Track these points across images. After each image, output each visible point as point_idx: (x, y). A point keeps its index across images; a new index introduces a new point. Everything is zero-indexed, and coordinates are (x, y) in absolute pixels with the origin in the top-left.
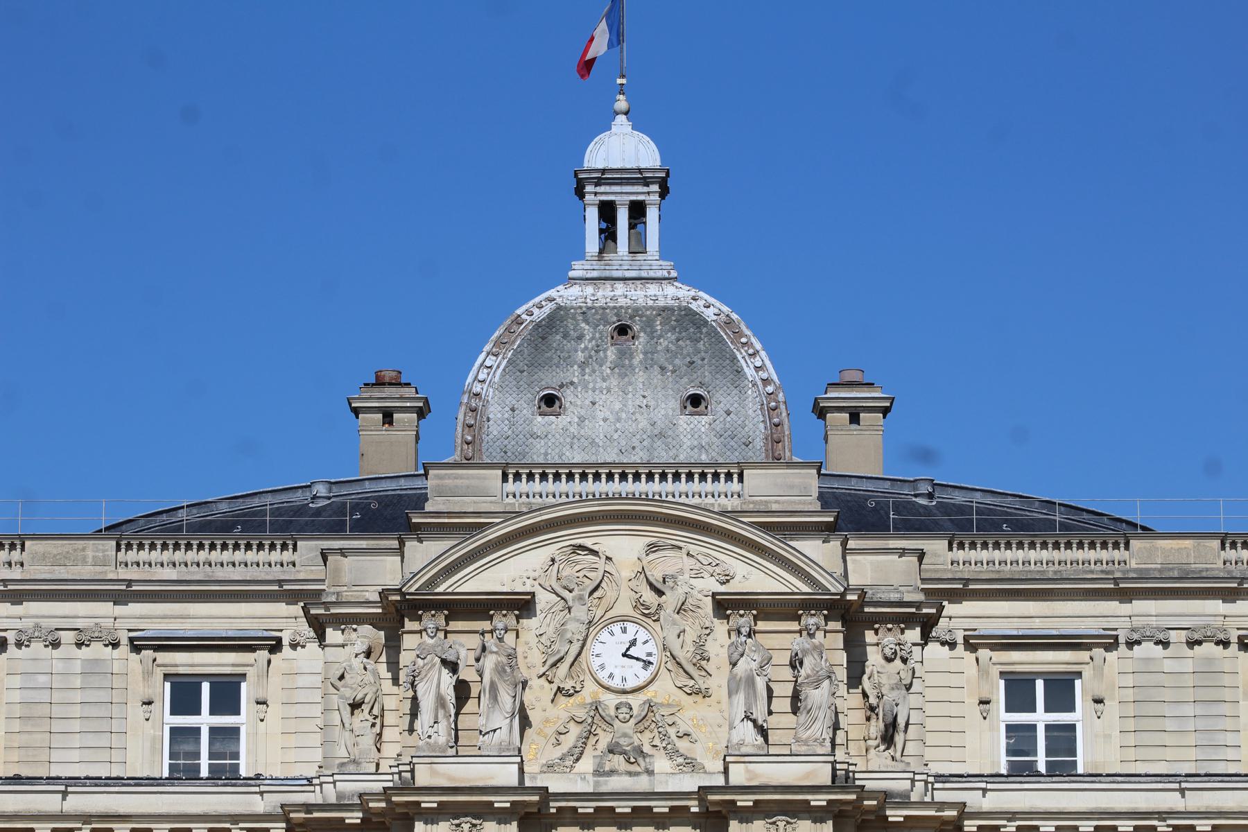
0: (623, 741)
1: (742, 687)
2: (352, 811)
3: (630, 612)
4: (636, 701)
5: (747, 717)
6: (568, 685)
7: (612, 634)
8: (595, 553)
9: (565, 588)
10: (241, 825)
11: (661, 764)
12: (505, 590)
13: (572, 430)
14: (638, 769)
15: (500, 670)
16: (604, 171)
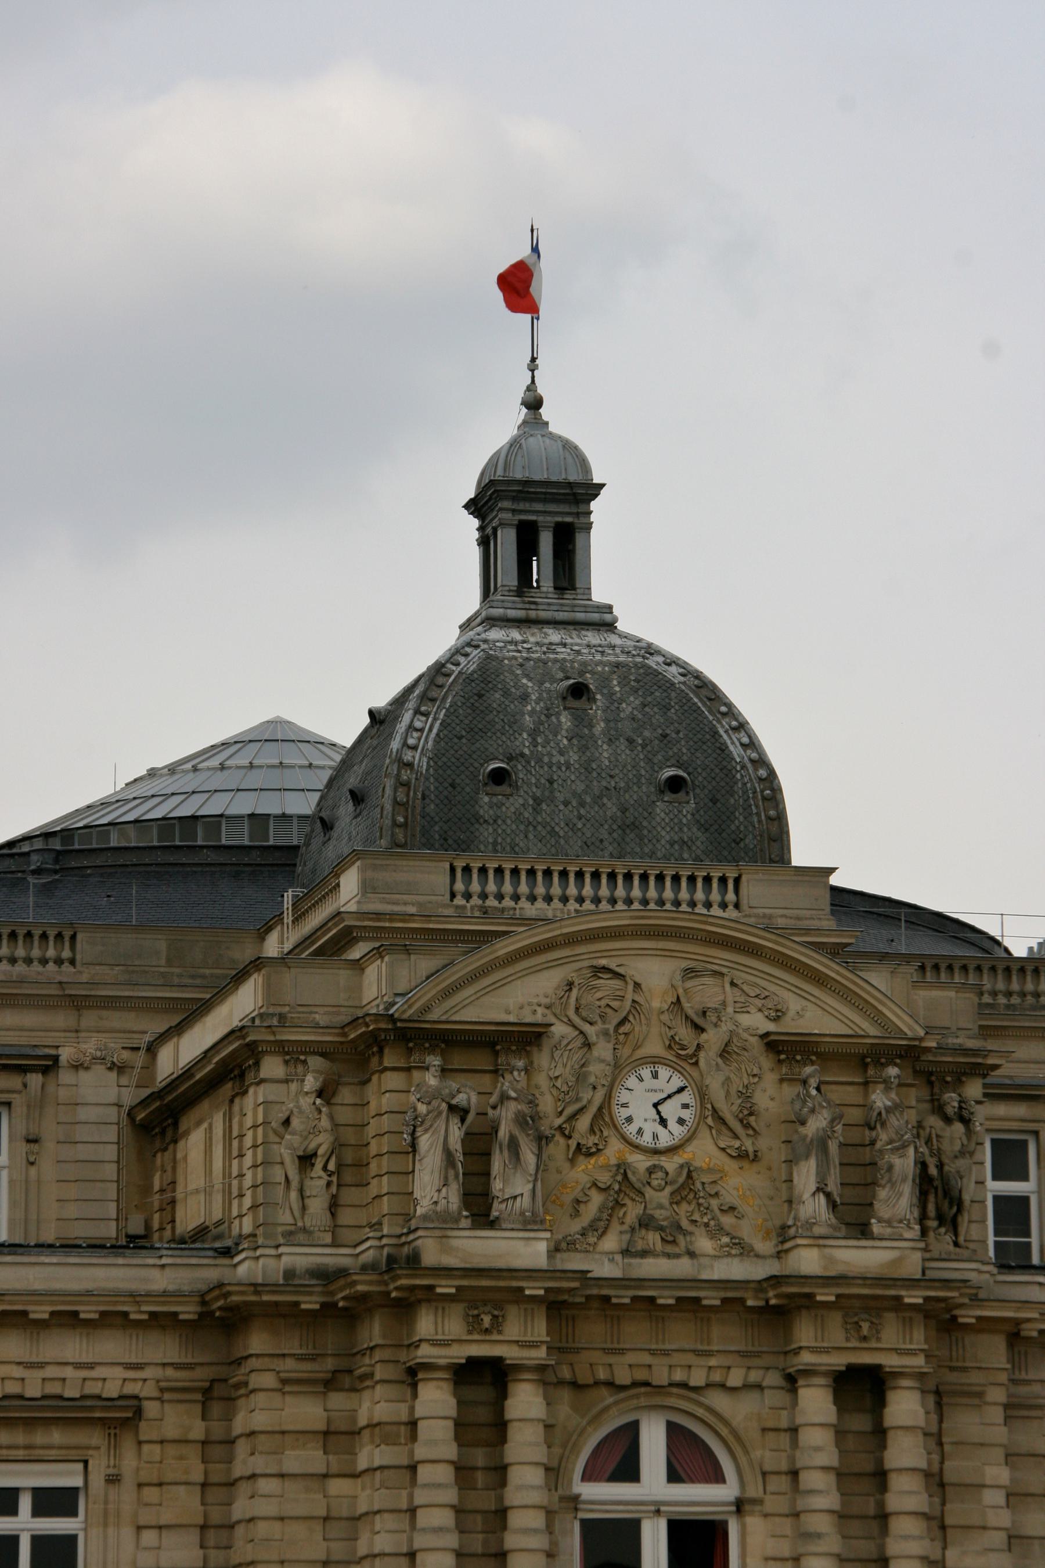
0: (658, 1214)
1: (814, 1152)
2: (310, 1294)
4: (671, 1164)
7: (641, 1080)
9: (584, 1020)
10: (144, 1308)
11: (704, 1244)
12: (512, 1019)
13: (526, 815)
14: (677, 1250)
15: (521, 1121)
16: (527, 483)
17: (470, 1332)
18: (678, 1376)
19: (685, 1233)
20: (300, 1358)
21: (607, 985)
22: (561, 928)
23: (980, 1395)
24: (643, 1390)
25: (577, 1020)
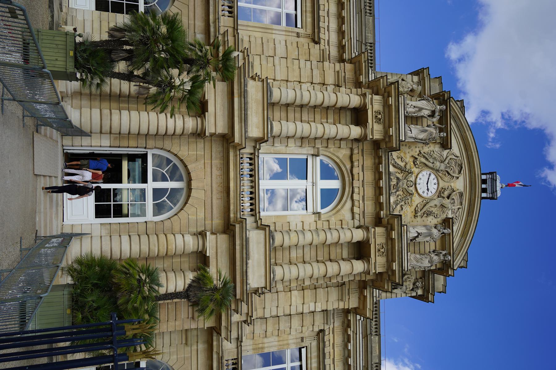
0: (401, 183)
2: (365, 78)
4: (412, 189)
6: (418, 162)
7: (434, 179)
8: (460, 172)
15: (431, 134)
17: (375, 112)
18: (356, 190)
19: (396, 192)
20: (345, 77)
21: (457, 169)
22: (475, 152)
23: (342, 300)
24: (351, 178)
25: (449, 158)
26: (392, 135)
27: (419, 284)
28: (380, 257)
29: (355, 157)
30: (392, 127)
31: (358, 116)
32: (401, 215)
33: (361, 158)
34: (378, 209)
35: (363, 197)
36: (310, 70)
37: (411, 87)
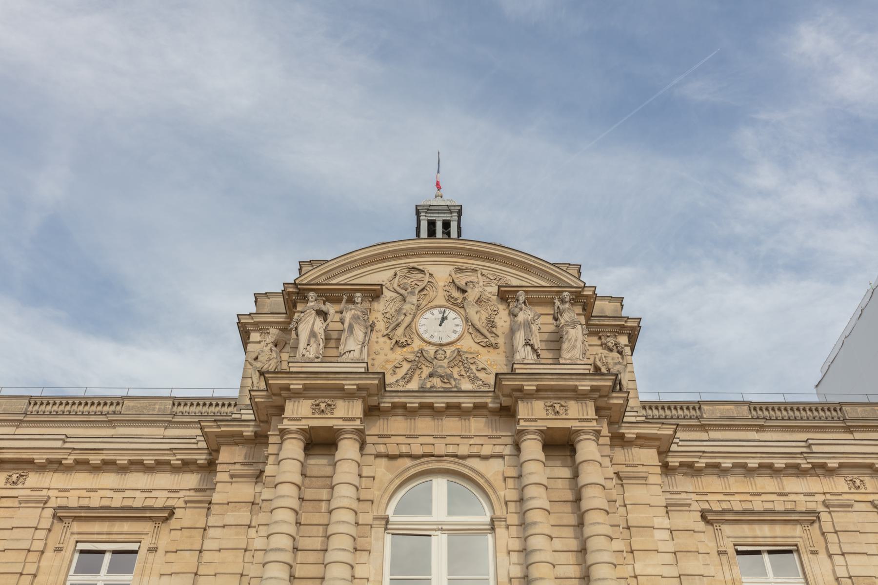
2: (248, 426)
3: (445, 303)
4: (449, 350)
5: (527, 344)
6: (403, 340)
7: (433, 314)
15: (355, 318)
17: (314, 413)
19: (455, 379)
20: (243, 464)
21: (418, 276)
23: (646, 478)
24: (430, 459)
26: (358, 385)
27: (611, 342)
28: (568, 412)
29: (393, 450)
30: (343, 385)
31: (320, 443)
32: (497, 374)
33: (393, 439)
34: (485, 412)
35: (463, 437)
36: (225, 530)
37: (271, 345)
